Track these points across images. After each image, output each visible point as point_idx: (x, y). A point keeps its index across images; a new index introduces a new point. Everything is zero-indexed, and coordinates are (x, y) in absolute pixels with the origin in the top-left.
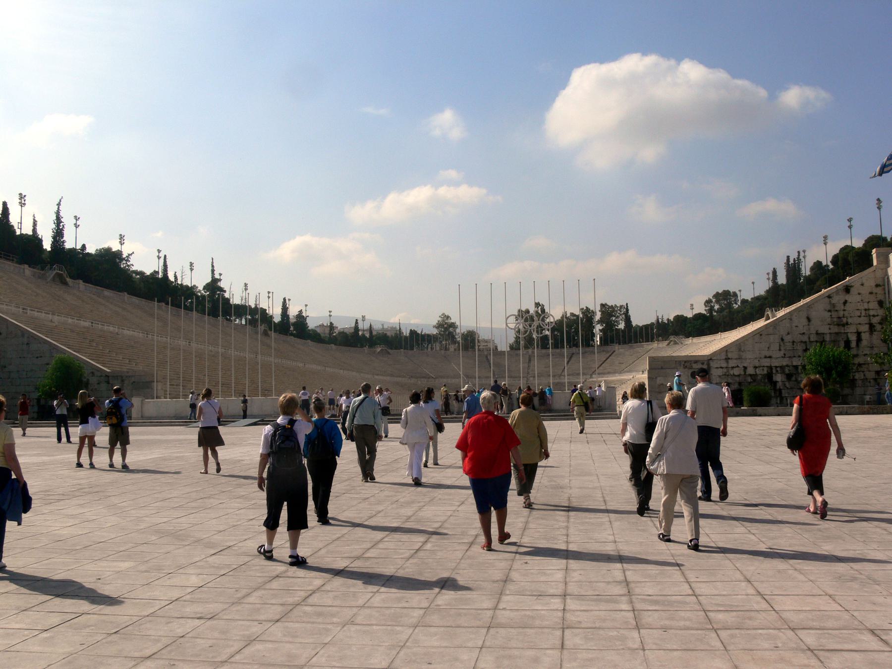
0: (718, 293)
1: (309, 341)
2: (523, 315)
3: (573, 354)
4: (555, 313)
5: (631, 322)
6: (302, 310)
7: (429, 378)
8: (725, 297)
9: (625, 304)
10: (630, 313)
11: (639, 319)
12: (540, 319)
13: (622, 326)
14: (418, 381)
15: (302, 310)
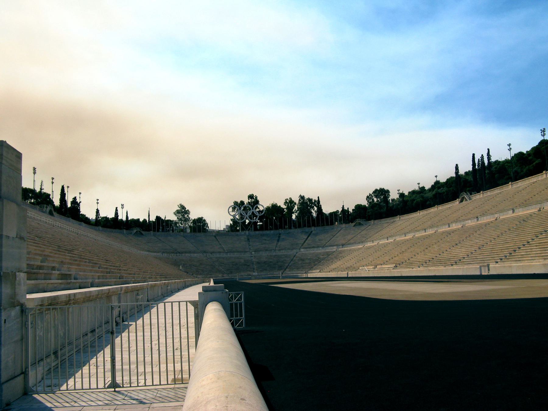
0: (376, 190)
1: (83, 223)
2: (238, 205)
3: (280, 234)
4: (264, 203)
5: (322, 210)
6: (75, 198)
7: (176, 253)
8: (382, 193)
9: (317, 199)
10: (321, 203)
11: (327, 209)
12: (254, 208)
13: (314, 214)
14: (169, 255)
15: (75, 197)
